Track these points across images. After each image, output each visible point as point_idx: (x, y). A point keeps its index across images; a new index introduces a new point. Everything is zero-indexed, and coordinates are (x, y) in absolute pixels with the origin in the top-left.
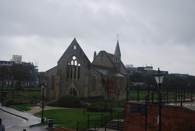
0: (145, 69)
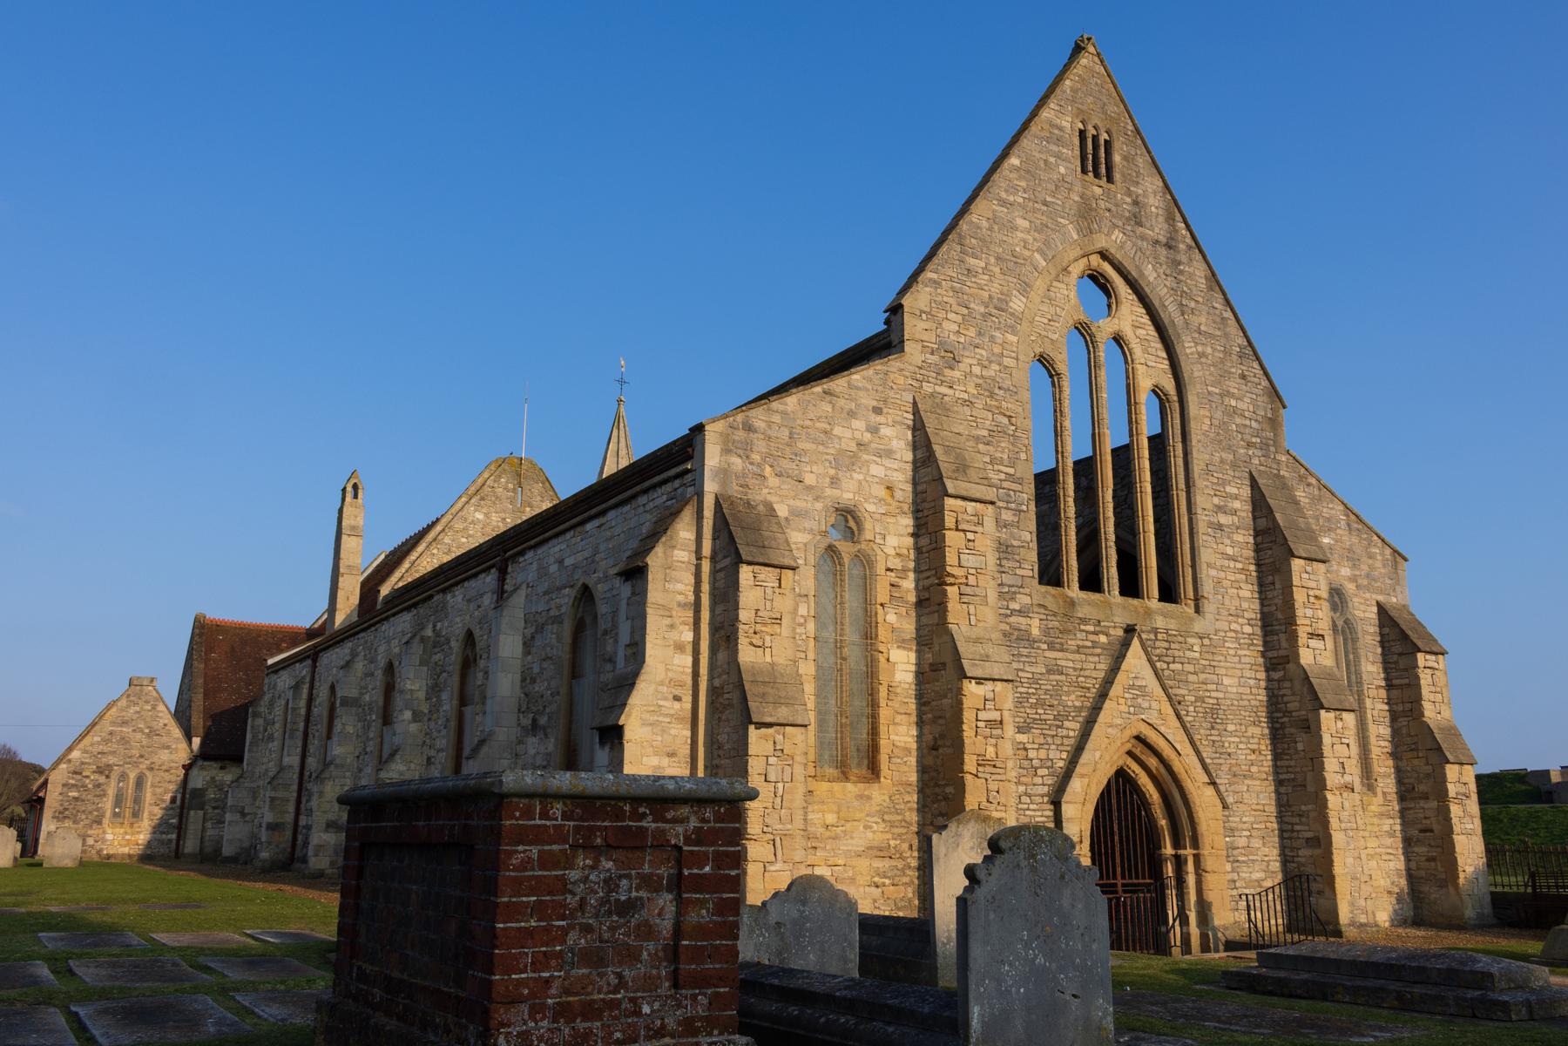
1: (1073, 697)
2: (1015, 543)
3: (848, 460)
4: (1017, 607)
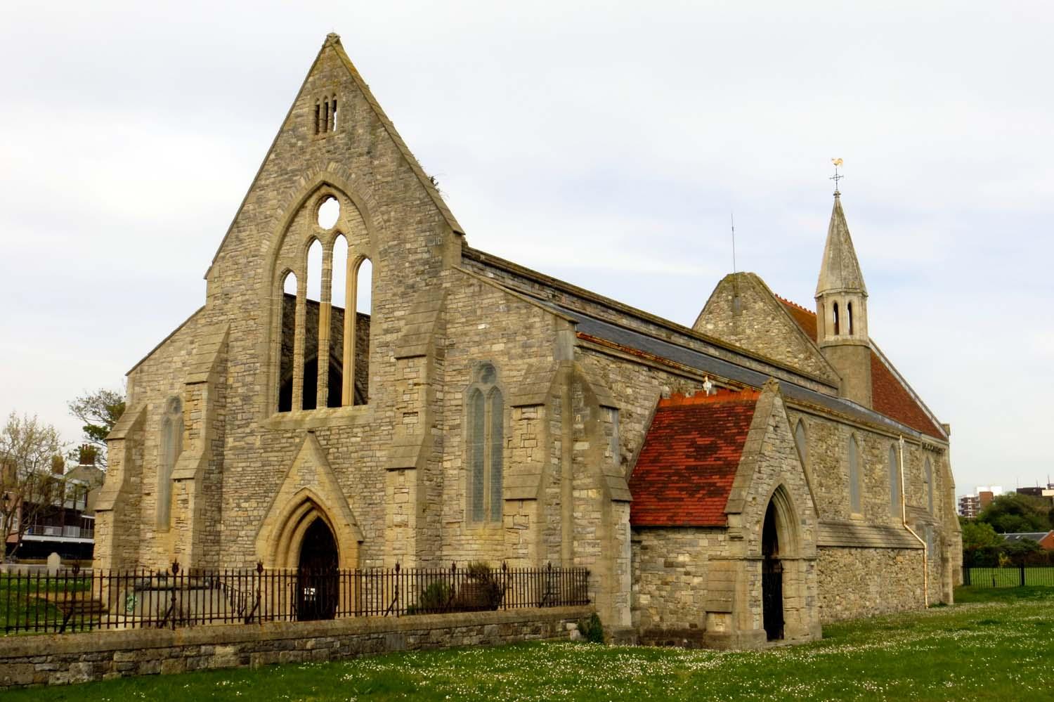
0: (1045, 493)
1: (276, 478)
2: (251, 394)
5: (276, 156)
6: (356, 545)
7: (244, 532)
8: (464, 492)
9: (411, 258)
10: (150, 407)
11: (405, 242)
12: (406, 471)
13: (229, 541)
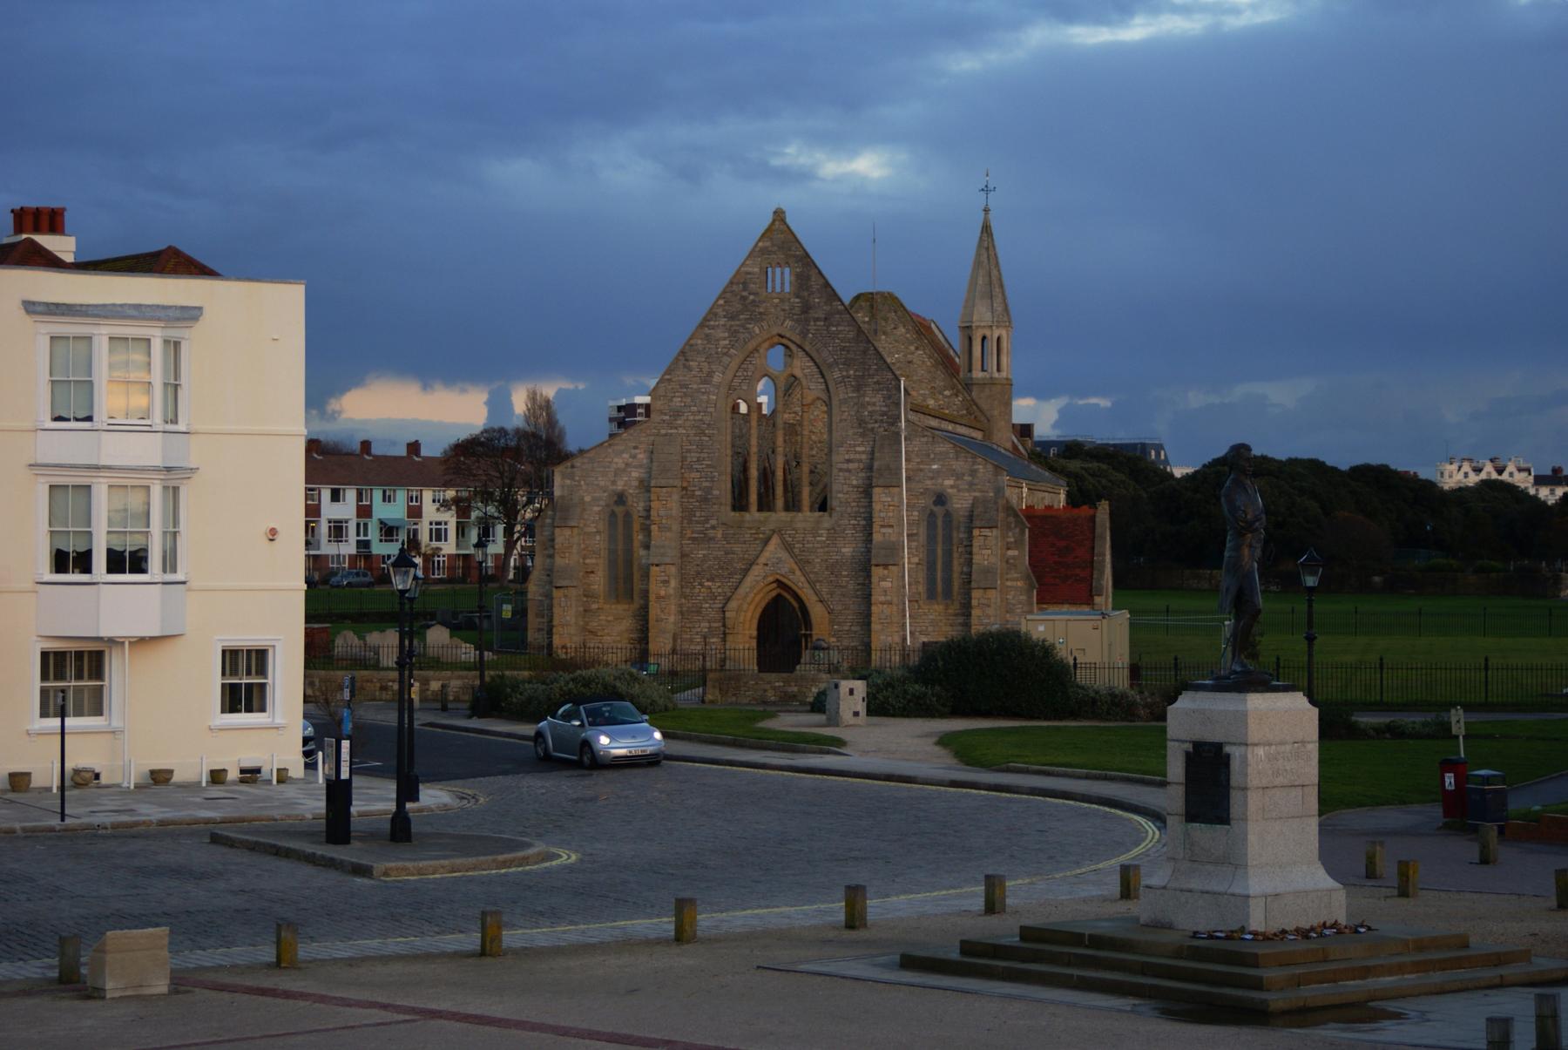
2: (709, 497)
3: (617, 472)
4: (709, 526)
5: (725, 302)
6: (827, 615)
7: (707, 605)
8: (921, 580)
9: (870, 408)
10: (587, 499)
11: (864, 396)
12: (890, 567)
13: (692, 612)
